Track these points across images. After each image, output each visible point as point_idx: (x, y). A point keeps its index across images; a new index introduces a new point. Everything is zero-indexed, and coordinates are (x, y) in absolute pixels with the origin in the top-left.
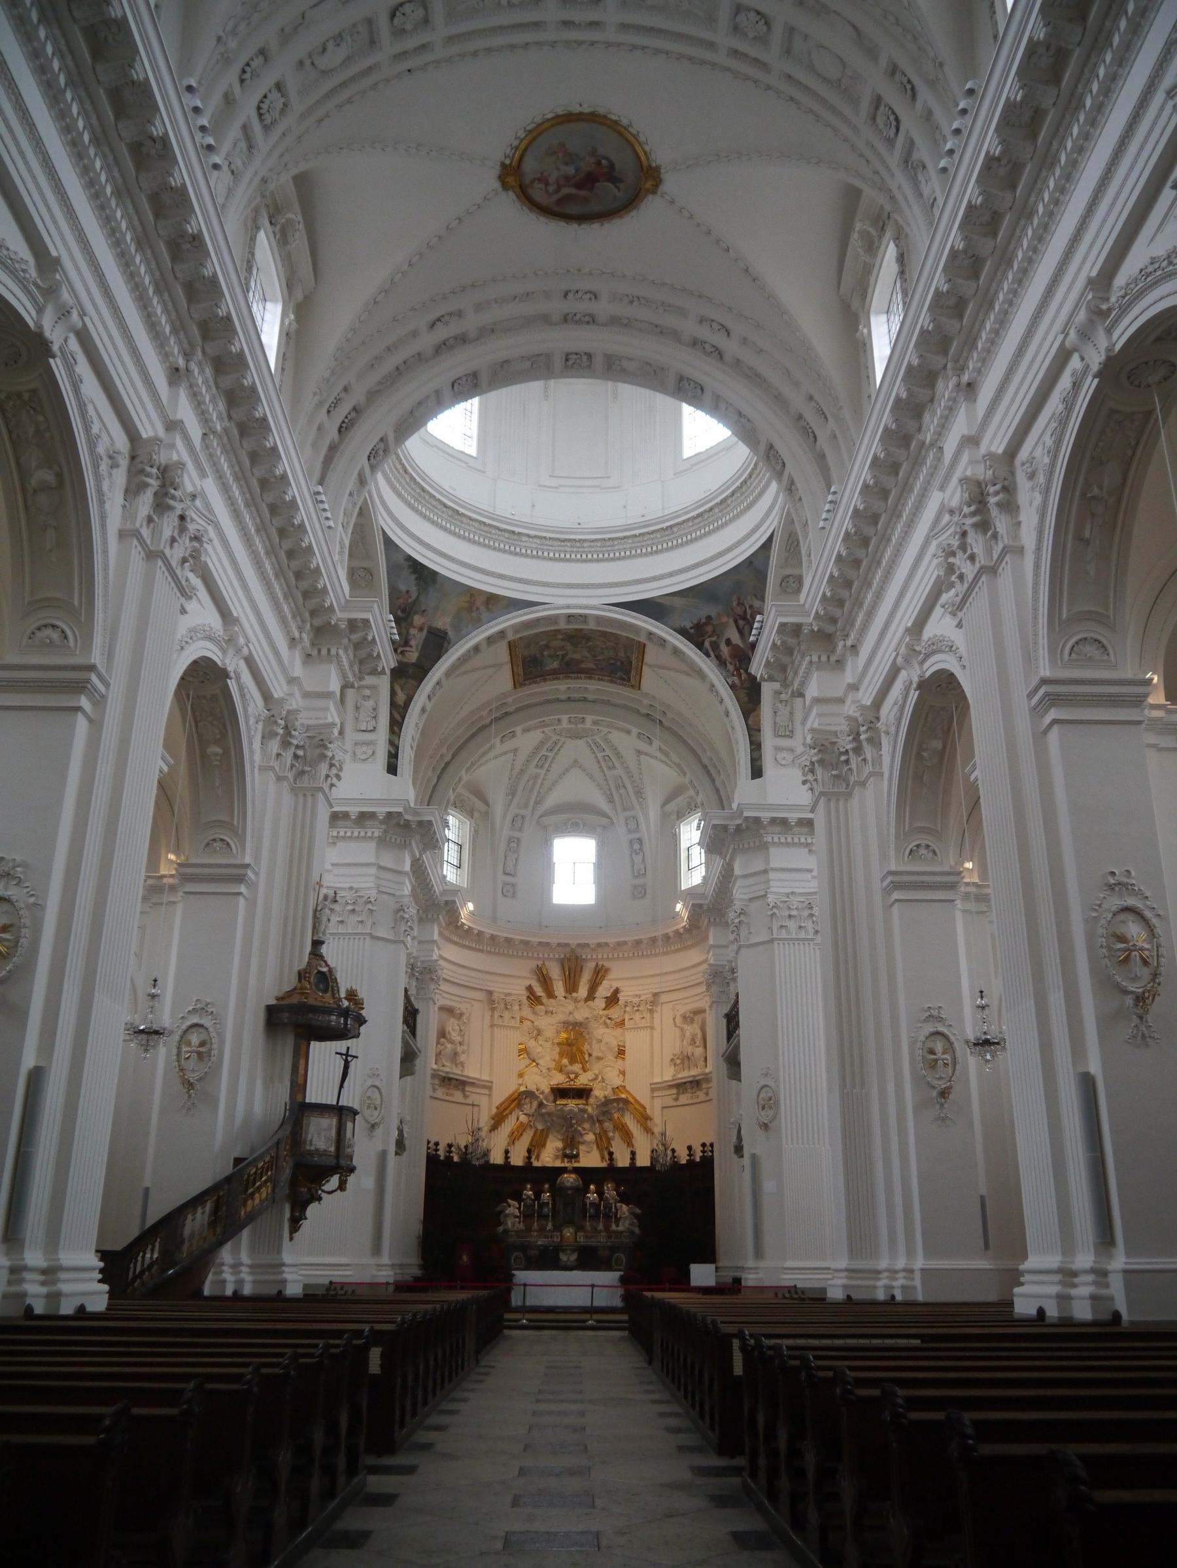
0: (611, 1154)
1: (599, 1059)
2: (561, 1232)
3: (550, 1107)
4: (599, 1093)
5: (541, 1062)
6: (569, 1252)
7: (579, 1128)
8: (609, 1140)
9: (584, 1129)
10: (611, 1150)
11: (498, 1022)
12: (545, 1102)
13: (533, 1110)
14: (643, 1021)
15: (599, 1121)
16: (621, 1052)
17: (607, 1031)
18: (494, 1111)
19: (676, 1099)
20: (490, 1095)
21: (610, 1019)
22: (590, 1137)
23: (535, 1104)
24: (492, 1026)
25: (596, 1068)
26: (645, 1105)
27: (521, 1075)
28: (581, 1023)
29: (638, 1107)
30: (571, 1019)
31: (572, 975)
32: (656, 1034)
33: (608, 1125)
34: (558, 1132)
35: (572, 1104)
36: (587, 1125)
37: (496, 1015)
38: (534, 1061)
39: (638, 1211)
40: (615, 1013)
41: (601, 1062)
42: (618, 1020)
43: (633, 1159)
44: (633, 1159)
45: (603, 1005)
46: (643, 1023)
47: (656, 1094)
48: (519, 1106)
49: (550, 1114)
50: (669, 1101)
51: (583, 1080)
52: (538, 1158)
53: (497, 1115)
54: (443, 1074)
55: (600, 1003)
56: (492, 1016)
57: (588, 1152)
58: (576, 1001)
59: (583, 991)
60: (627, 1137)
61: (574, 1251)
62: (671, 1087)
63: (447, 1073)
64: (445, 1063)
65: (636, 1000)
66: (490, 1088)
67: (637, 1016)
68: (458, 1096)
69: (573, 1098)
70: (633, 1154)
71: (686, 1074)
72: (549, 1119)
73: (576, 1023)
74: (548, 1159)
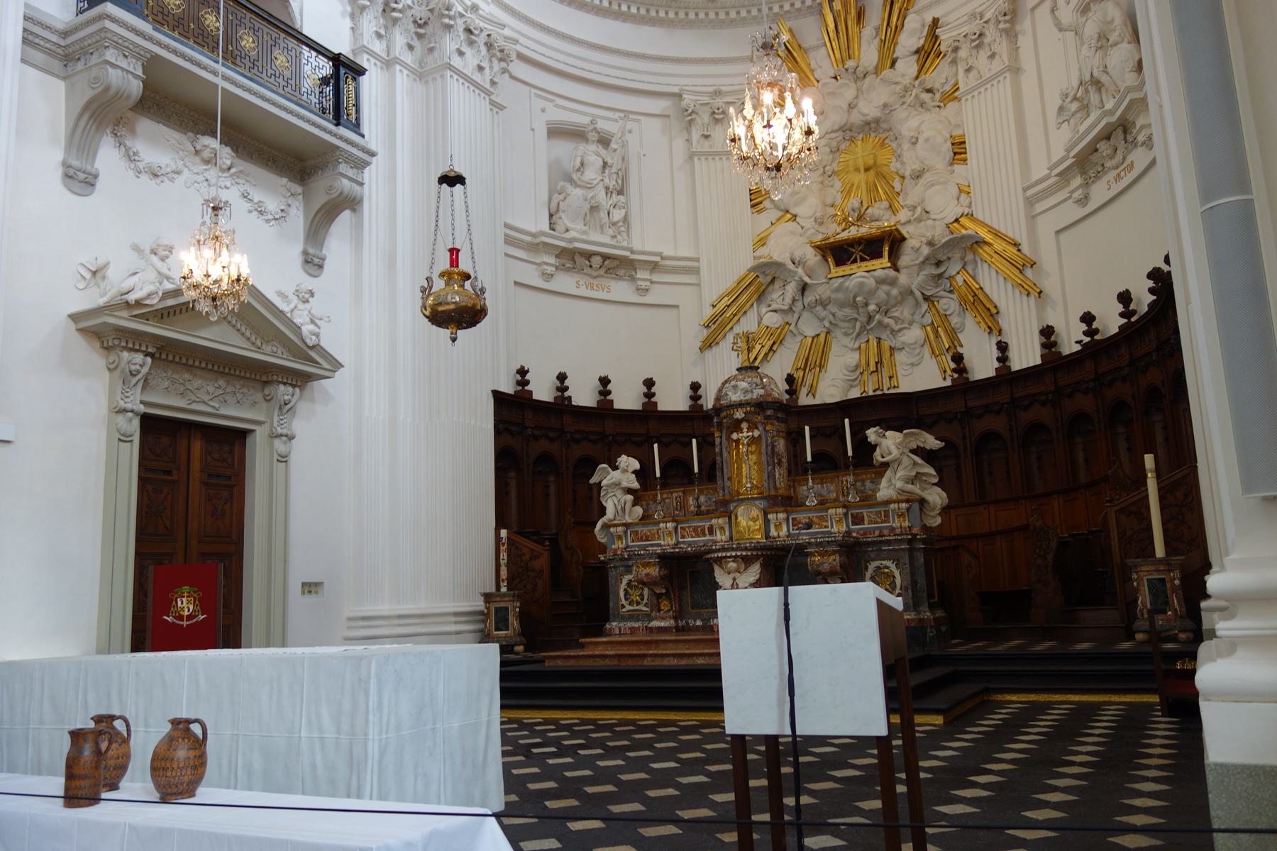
0: (958, 358)
1: (917, 176)
2: (730, 515)
3: (822, 290)
4: (917, 238)
5: (800, 210)
6: (732, 565)
7: (887, 320)
8: (953, 334)
9: (896, 319)
10: (960, 350)
11: (706, 146)
12: (807, 279)
13: (788, 300)
14: (997, 60)
15: (926, 298)
16: (959, 150)
17: (927, 117)
18: (708, 312)
19: (1084, 200)
20: (698, 285)
21: (929, 91)
22: (914, 334)
23: (791, 289)
24: (691, 156)
25: (913, 194)
26: (1018, 240)
27: (762, 242)
28: (877, 121)
29: (999, 245)
30: (856, 118)
31: (842, 27)
32: (1028, 82)
33: (949, 304)
34: (846, 334)
35: (862, 274)
36: (904, 312)
37: (695, 136)
38: (787, 211)
39: (932, 442)
40: (939, 75)
41: (922, 181)
42: (948, 88)
43: (1003, 359)
44: (1003, 359)
45: (914, 70)
46: (997, 65)
47: (1040, 207)
48: (761, 296)
49: (823, 303)
50: (1073, 212)
51: (882, 219)
52: (812, 391)
53: (713, 320)
54: (563, 244)
55: (907, 67)
56: (689, 141)
57: (913, 365)
58: (859, 76)
59: (868, 54)
60: (990, 316)
61: (748, 561)
62: (1065, 176)
63: (571, 241)
64: (570, 225)
65: (974, 27)
66: (696, 271)
67: (981, 60)
68: (620, 289)
69: (863, 260)
70: (1003, 347)
71: (1092, 124)
72: (823, 313)
73: (868, 123)
74: (833, 391)
